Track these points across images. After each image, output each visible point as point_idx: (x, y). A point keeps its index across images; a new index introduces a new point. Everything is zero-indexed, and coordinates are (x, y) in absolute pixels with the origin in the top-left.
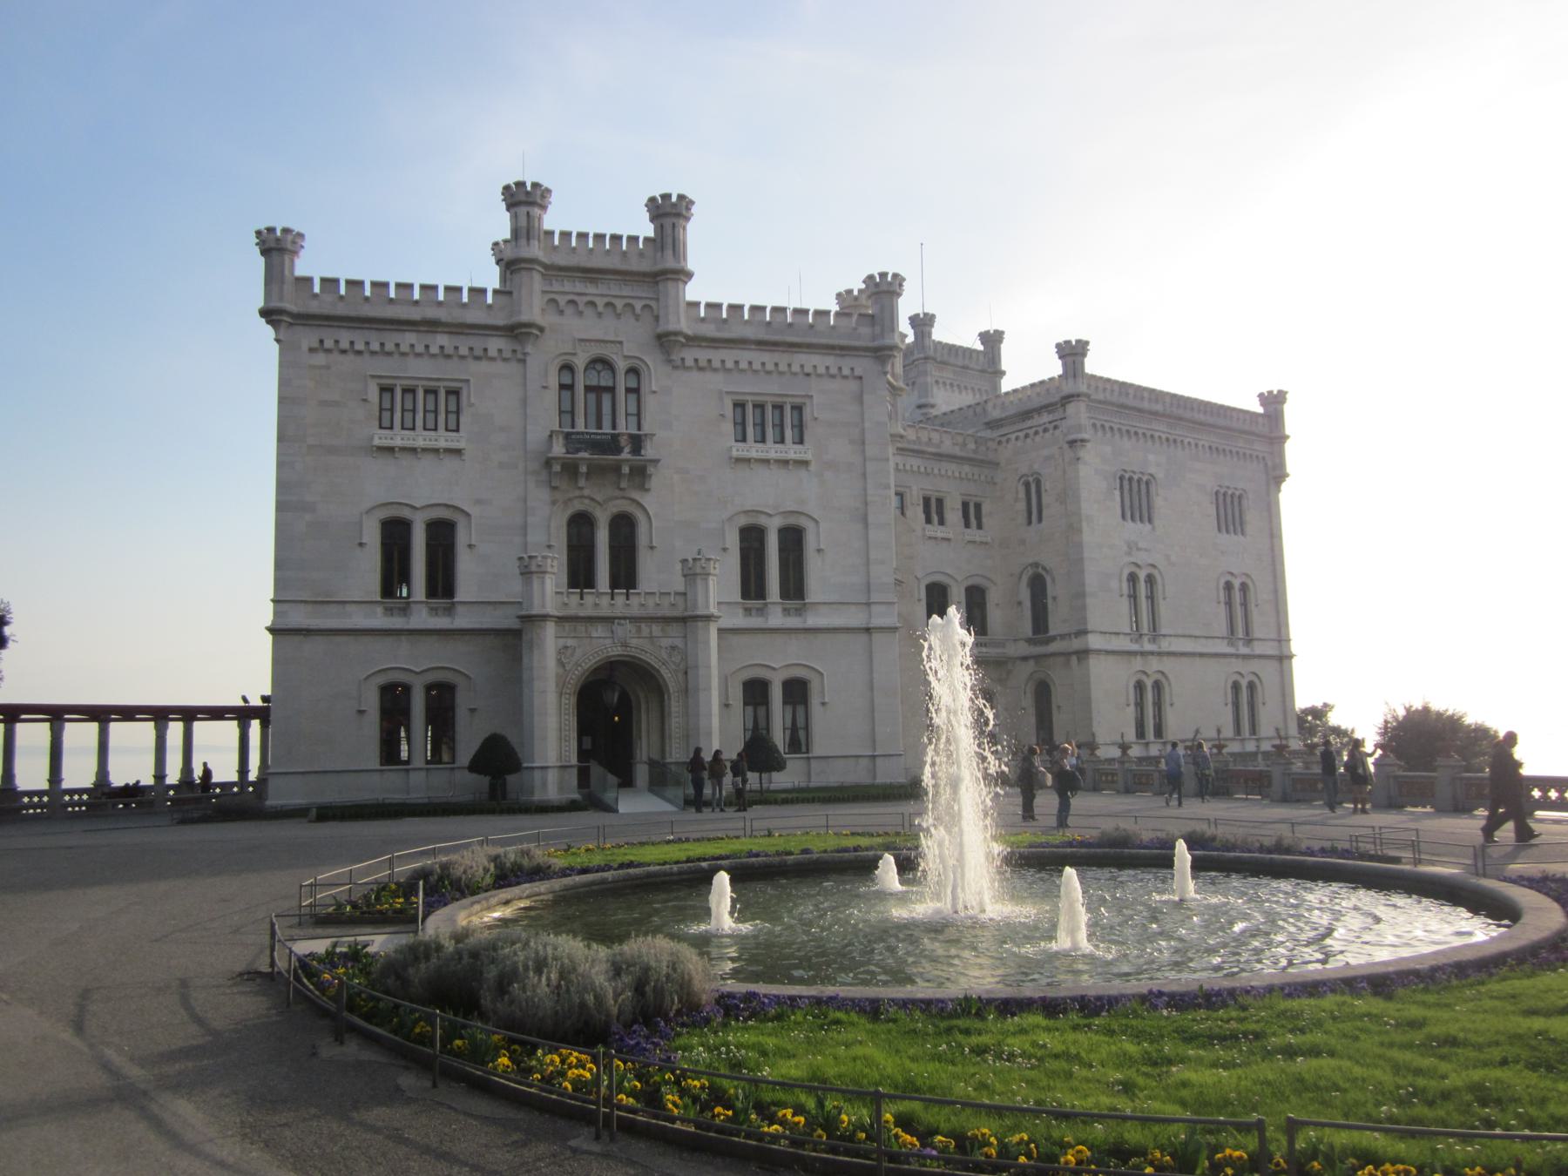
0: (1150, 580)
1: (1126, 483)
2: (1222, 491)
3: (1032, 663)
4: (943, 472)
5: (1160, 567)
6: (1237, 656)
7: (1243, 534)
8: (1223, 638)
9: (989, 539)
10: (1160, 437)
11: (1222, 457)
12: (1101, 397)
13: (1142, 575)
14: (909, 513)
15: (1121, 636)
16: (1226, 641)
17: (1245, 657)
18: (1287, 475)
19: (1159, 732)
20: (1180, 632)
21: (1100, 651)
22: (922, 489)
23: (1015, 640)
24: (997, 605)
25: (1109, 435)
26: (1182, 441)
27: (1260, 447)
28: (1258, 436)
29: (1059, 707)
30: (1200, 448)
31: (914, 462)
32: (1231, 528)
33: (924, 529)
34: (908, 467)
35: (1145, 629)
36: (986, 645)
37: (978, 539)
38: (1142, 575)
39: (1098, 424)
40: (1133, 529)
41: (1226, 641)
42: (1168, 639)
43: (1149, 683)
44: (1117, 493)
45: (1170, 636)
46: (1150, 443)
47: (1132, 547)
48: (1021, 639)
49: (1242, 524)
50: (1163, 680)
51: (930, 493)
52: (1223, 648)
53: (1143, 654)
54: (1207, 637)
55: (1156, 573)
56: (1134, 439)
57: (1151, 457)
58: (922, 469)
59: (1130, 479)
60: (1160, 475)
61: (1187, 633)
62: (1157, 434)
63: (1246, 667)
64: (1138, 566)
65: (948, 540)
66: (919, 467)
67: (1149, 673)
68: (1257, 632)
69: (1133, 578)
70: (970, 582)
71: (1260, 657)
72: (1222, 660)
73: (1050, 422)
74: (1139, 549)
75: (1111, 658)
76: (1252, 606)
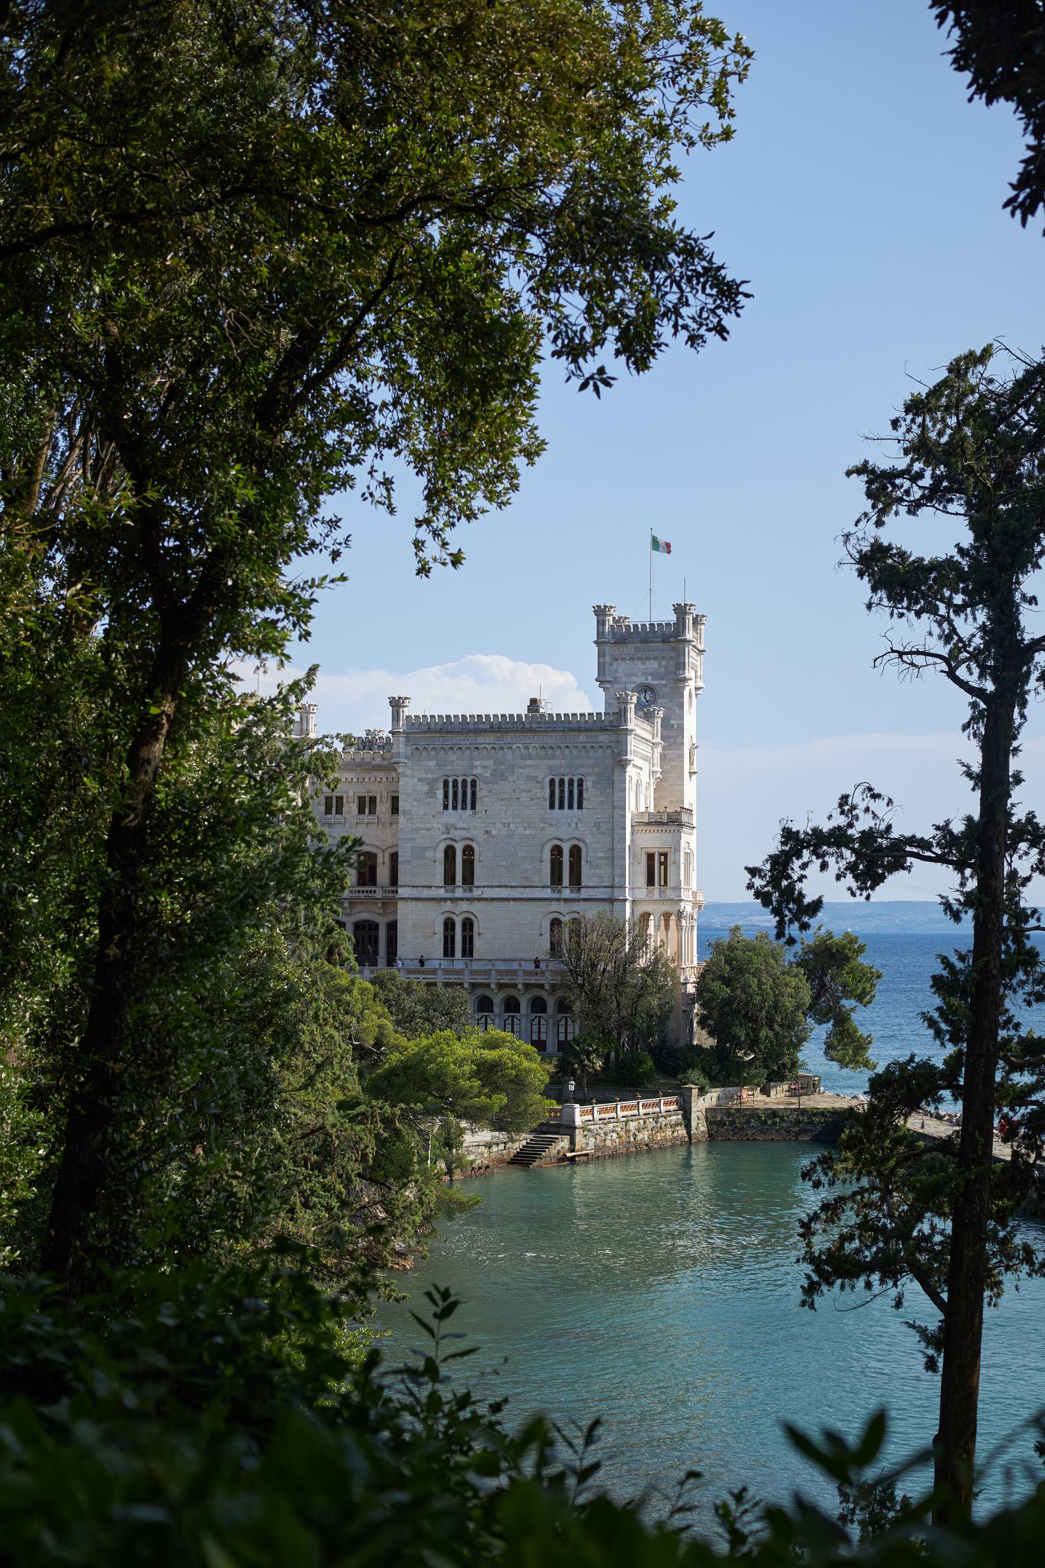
0: (469, 851)
6: (558, 900)
11: (558, 752)
13: (459, 847)
25: (433, 753)
27: (604, 738)
38: (459, 847)
40: (452, 816)
44: (440, 794)
46: (476, 753)
47: (448, 829)
52: (548, 893)
53: (451, 899)
55: (474, 845)
57: (477, 763)
59: (455, 782)
68: (584, 882)
71: (584, 900)
75: (420, 904)
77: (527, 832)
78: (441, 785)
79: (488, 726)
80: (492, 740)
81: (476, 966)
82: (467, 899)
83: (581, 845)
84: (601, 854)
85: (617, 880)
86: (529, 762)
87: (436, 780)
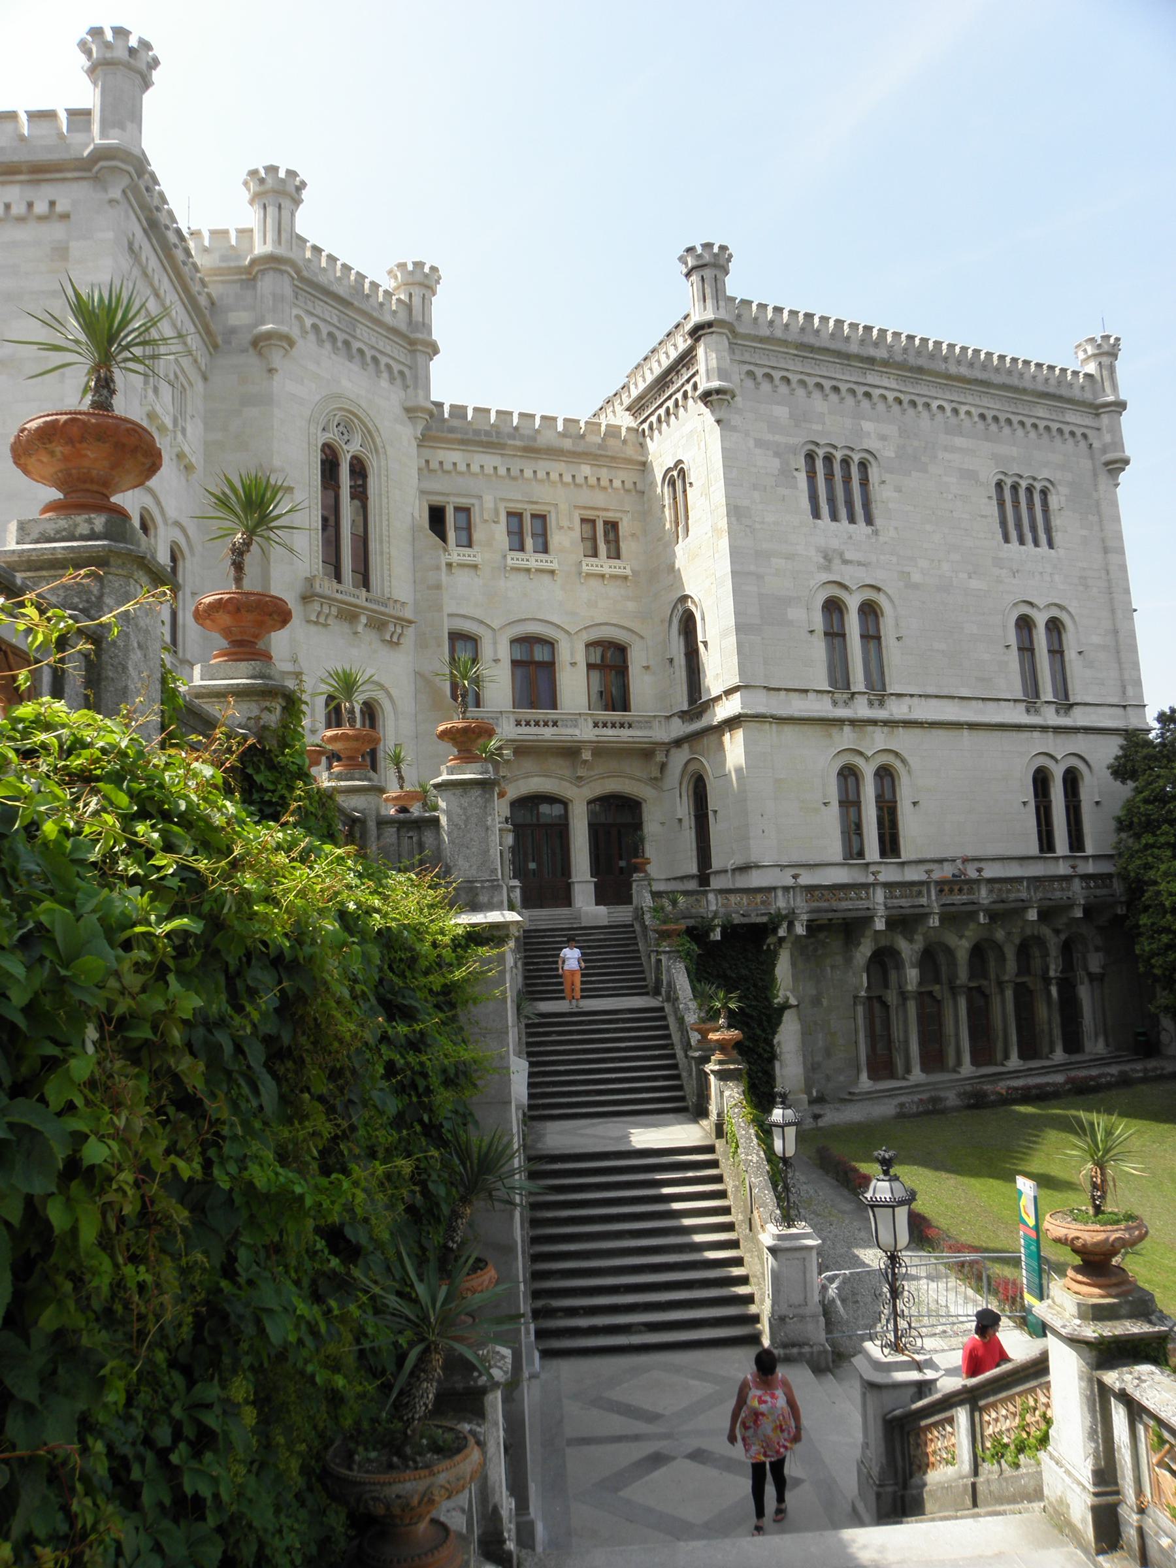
0: (869, 610)
1: (819, 465)
2: (1009, 482)
3: (686, 746)
4: (541, 475)
5: (889, 592)
6: (1044, 729)
7: (1051, 545)
8: (1015, 701)
9: (628, 572)
10: (884, 397)
11: (1007, 430)
12: (765, 332)
13: (853, 603)
14: (476, 536)
15: (811, 695)
16: (1022, 706)
17: (1058, 730)
18: (1126, 462)
19: (890, 844)
20: (931, 690)
21: (763, 716)
22: (502, 500)
23: (668, 718)
24: (647, 668)
25: (783, 389)
26: (927, 405)
28: (1070, 401)
29: (715, 812)
30: (962, 415)
31: (490, 461)
32: (1029, 536)
33: (505, 557)
34: (475, 468)
35: (858, 682)
36: (614, 726)
37: (606, 570)
38: (853, 603)
39: (759, 372)
41: (1022, 706)
42: (908, 698)
43: (868, 771)
44: (802, 478)
45: (912, 696)
46: (865, 403)
47: (828, 558)
48: (673, 715)
49: (1048, 530)
50: (898, 764)
51: (526, 506)
52: (1017, 715)
53: (853, 722)
54: (983, 699)
55: (881, 599)
56: (834, 397)
57: (867, 426)
58: (502, 471)
59: (828, 459)
60: (887, 452)
61: (945, 692)
62: (876, 392)
63: (1061, 747)
64: (844, 587)
65: (552, 572)
66: (495, 468)
67: (869, 754)
69: (833, 607)
70: (595, 635)
72: (1014, 735)
73: (688, 381)
74: (846, 562)
75: (789, 731)
76: (1071, 655)
77: (974, 584)
78: (801, 462)
79: (882, 353)
80: (894, 385)
81: (913, 875)
82: (886, 723)
83: (1064, 617)
84: (1095, 639)
85: (1130, 691)
86: (959, 441)
87: (794, 450)
